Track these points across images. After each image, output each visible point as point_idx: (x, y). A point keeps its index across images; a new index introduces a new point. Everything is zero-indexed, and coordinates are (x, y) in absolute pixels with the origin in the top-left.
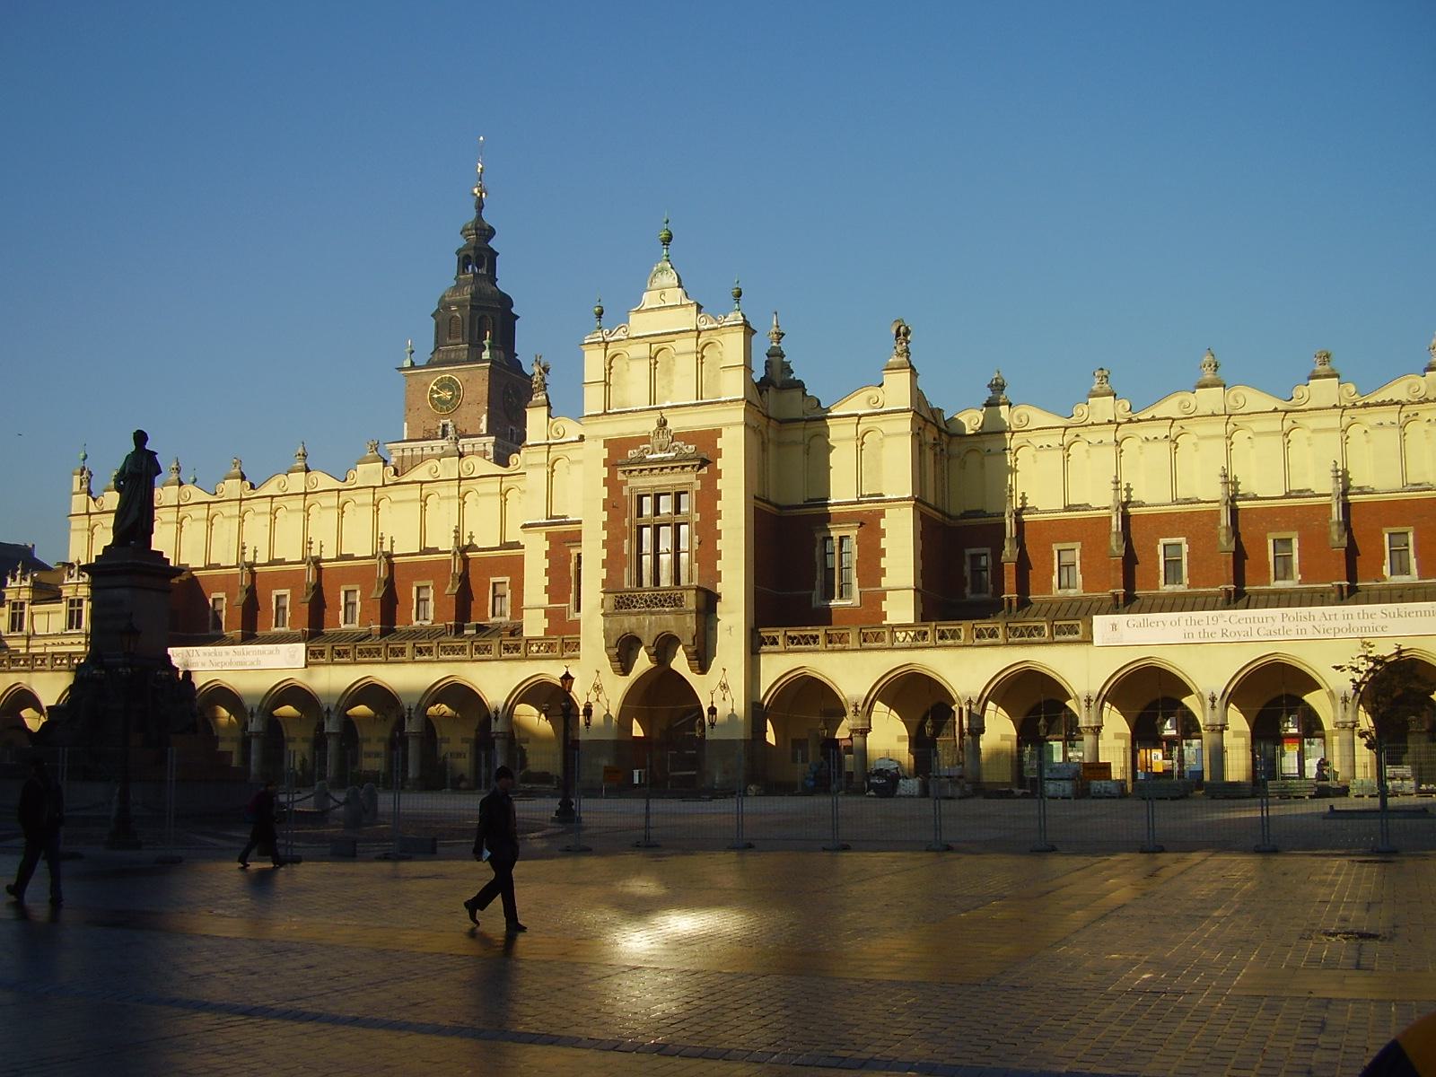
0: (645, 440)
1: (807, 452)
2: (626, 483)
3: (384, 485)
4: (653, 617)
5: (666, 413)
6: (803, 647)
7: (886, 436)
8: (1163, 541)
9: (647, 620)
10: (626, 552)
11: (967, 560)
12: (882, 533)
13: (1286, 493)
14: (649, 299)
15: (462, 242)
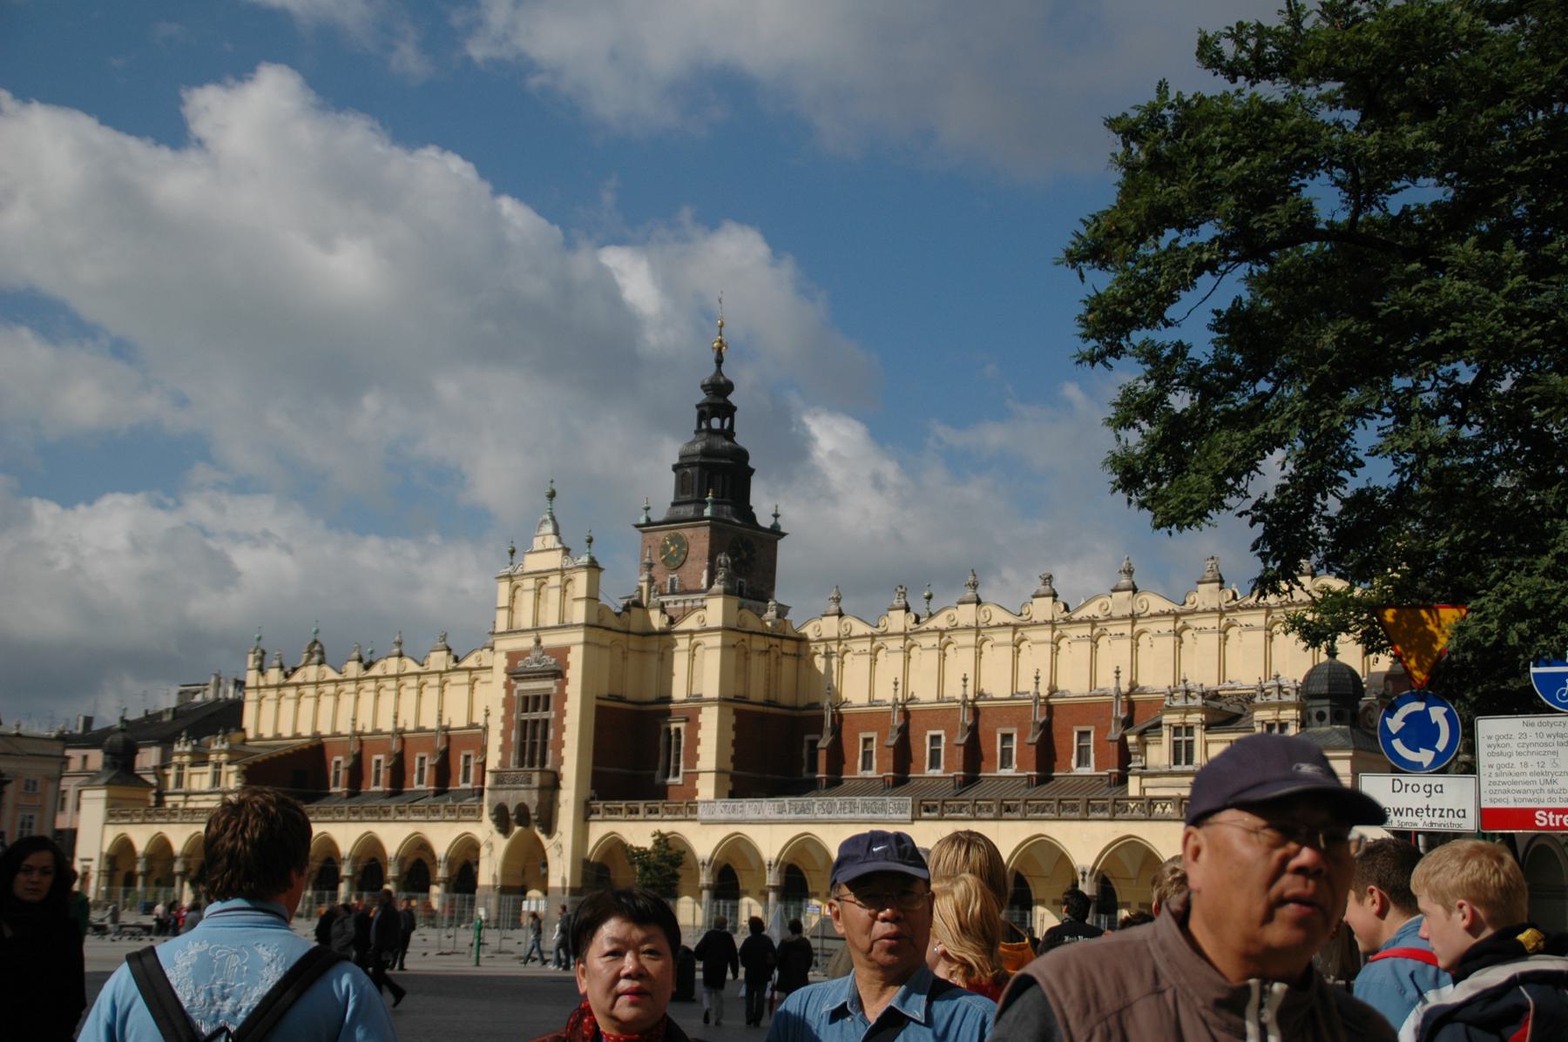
0: (526, 653)
1: (662, 659)
2: (515, 686)
3: (448, 671)
4: (515, 792)
5: (541, 633)
6: (613, 816)
7: (706, 649)
8: (930, 733)
9: (512, 793)
10: (513, 739)
11: (806, 744)
12: (697, 726)
13: (1012, 694)
14: (537, 543)
15: (702, 397)
